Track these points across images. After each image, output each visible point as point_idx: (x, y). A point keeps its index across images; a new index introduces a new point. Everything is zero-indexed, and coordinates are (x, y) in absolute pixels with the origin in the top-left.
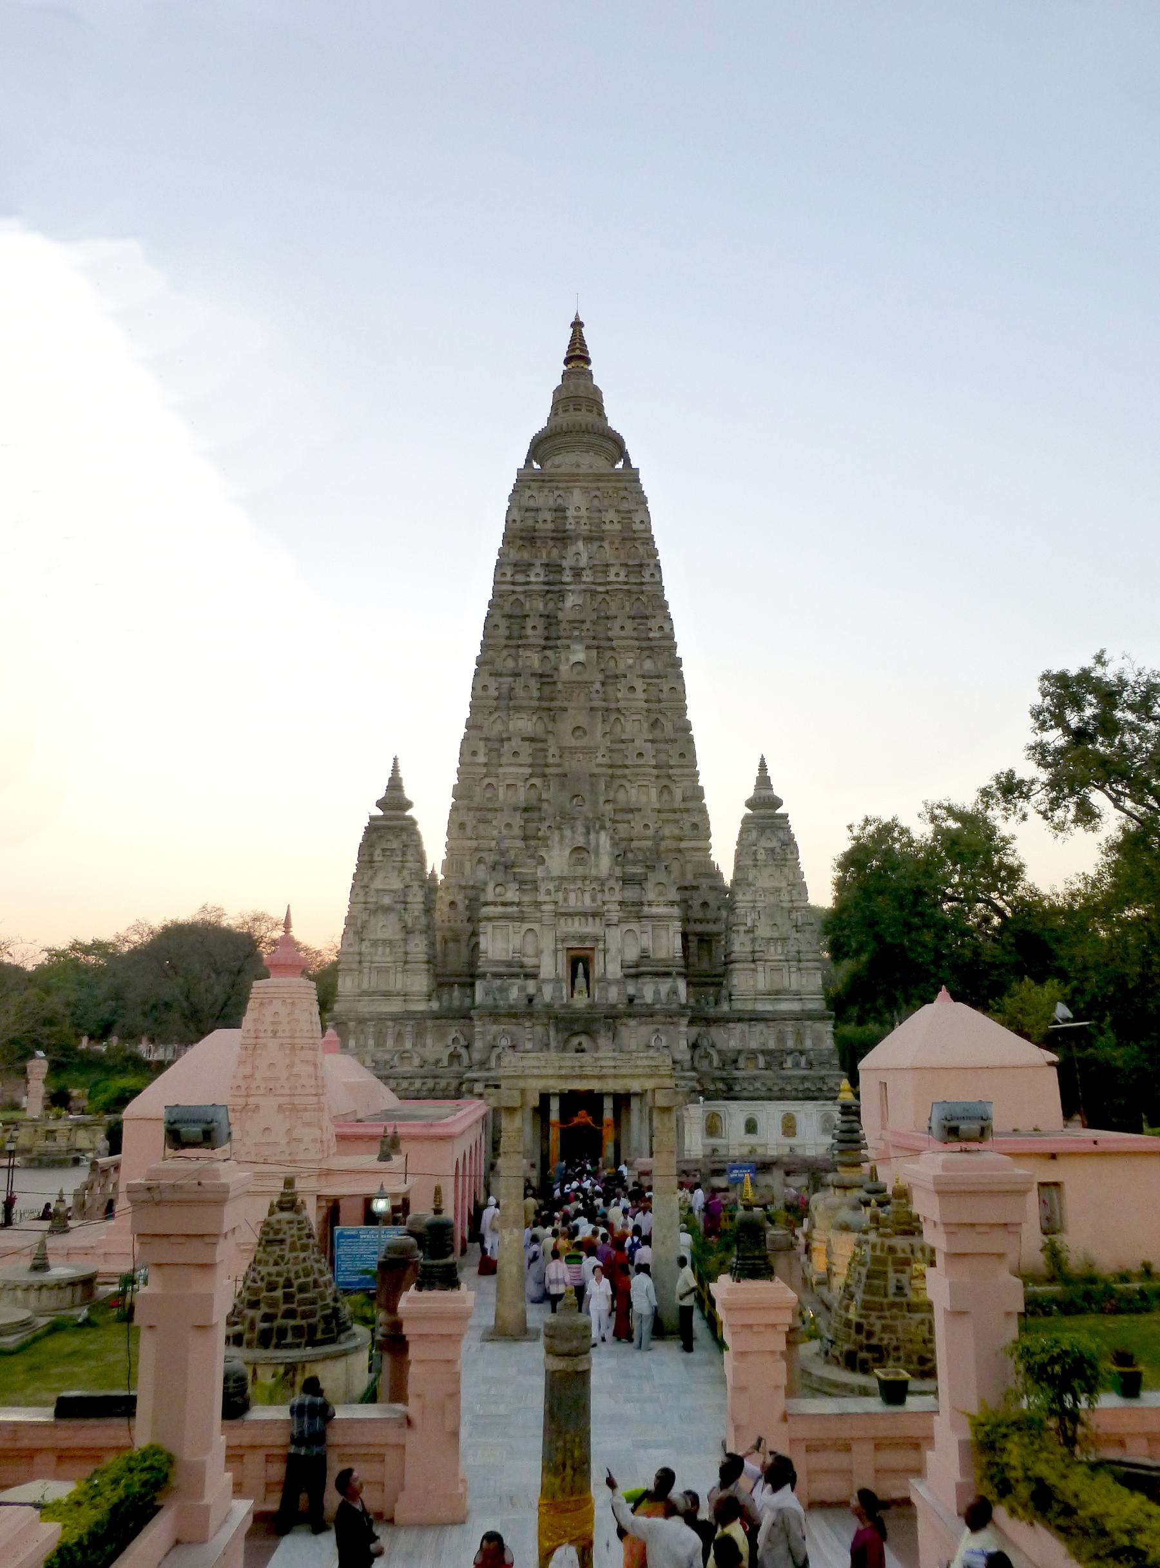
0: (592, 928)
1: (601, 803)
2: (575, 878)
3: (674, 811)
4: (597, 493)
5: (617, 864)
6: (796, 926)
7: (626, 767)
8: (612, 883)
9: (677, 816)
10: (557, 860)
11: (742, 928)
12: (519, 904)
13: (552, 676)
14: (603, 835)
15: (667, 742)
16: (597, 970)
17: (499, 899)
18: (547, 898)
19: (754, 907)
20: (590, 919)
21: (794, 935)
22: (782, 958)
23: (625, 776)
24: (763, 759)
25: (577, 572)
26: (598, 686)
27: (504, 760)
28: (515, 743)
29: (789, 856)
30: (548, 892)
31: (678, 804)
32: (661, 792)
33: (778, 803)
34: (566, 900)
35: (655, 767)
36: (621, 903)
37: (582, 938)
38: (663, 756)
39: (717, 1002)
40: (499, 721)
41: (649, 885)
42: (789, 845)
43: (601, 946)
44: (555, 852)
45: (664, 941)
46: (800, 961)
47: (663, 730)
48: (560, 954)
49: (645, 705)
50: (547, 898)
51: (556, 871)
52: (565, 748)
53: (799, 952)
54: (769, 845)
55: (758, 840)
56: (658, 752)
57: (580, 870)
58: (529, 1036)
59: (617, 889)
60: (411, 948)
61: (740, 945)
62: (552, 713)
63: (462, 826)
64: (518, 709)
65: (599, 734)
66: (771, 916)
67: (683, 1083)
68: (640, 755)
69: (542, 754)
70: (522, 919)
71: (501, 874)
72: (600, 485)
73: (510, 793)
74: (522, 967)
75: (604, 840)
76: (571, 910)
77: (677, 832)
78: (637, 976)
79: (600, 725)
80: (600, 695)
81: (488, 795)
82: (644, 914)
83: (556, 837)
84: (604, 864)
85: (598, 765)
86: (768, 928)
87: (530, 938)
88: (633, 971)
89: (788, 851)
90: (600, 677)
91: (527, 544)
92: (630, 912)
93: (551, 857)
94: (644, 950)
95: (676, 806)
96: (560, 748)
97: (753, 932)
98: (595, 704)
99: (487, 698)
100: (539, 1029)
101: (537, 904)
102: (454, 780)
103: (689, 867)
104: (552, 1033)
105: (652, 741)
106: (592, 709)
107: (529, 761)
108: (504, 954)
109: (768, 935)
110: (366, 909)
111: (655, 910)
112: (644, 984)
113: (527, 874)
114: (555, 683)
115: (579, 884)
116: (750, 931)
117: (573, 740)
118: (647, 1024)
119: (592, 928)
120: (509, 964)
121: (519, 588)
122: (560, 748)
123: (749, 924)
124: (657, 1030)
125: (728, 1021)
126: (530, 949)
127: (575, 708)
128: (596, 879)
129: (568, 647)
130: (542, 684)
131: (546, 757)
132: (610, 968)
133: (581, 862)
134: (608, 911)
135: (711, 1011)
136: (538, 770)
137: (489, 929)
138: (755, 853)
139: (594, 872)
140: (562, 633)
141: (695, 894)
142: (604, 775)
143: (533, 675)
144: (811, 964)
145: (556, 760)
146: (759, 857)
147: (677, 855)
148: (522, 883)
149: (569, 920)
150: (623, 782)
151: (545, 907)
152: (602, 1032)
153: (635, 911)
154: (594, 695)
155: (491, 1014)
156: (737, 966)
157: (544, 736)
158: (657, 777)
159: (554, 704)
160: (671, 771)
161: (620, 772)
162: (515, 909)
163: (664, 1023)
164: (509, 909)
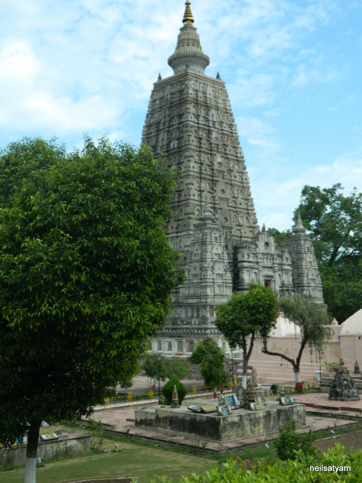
0: (270, 273)
4: (214, 89)
8: (276, 257)
13: (211, 166)
17: (248, 260)
22: (314, 285)
25: (214, 123)
37: (268, 276)
44: (261, 243)
51: (262, 252)
60: (227, 278)
72: (215, 86)
91: (196, 105)
95: (252, 225)
106: (226, 183)
110: (212, 261)
121: (196, 125)
129: (216, 155)
139: (271, 252)
140: (213, 149)
151: (260, 264)
164: (251, 264)
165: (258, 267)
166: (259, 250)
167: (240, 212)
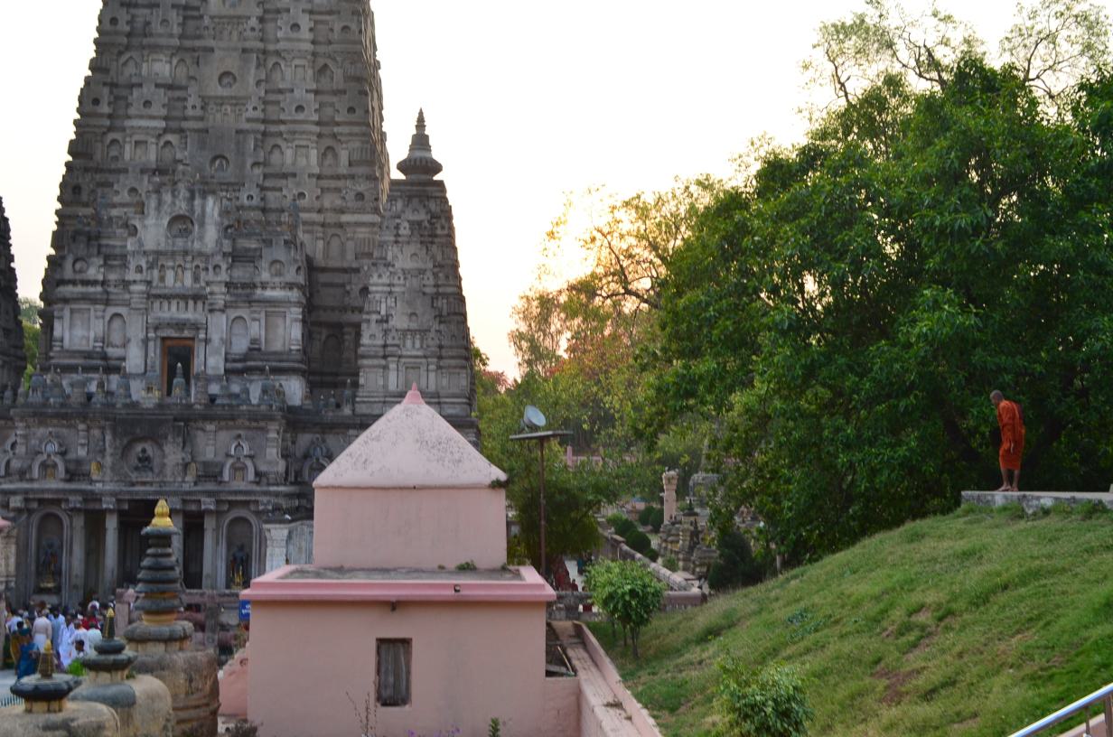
0: (191, 314)
1: (248, 165)
2: (173, 253)
3: (338, 177)
5: (225, 237)
6: (440, 316)
7: (283, 122)
8: (218, 259)
9: (340, 184)
10: (153, 232)
11: (374, 317)
12: (103, 283)
13: (197, 9)
14: (210, 201)
15: (336, 93)
16: (197, 365)
17: (78, 277)
18: (138, 277)
19: (390, 293)
20: (191, 303)
21: (436, 326)
22: (420, 353)
23: (281, 134)
24: (421, 113)
26: (253, 22)
27: (132, 111)
28: (148, 90)
29: (439, 232)
30: (139, 269)
31: (343, 170)
32: (324, 155)
33: (437, 168)
34: (162, 279)
35: (318, 123)
36: (227, 285)
37: (180, 325)
38: (329, 111)
39: (338, 406)
40: (131, 64)
41: (264, 264)
42: (446, 214)
43: (202, 336)
44: (150, 221)
45: (280, 331)
46: (440, 358)
47: (332, 79)
48: (151, 344)
49: (309, 47)
50: (138, 277)
51: (150, 245)
52: (210, 98)
53: (441, 347)
54: (416, 217)
55: (404, 212)
56: (322, 105)
57: (180, 243)
58: (83, 441)
59: (224, 266)
61: (370, 337)
62: (196, 54)
63: (77, 189)
64: (155, 48)
65: (252, 81)
66: (409, 303)
67: (265, 499)
68: (300, 108)
69: (179, 104)
70: (107, 303)
71: (82, 246)
73: (139, 151)
74: (105, 357)
75: (212, 207)
76: (166, 291)
77: (338, 202)
78: (239, 372)
79: (253, 71)
80: (256, 34)
81: (114, 153)
82: (256, 297)
83: (153, 203)
84: (210, 236)
85: (248, 120)
86: (405, 318)
87: (117, 324)
88: (239, 365)
89: (438, 226)
90: (259, 12)
92: (240, 295)
93: (145, 227)
94: (254, 341)
96: (203, 98)
97: (387, 321)
98: (248, 45)
99: (116, 33)
100: (96, 432)
101: (126, 284)
102: (70, 133)
103: (350, 245)
104: (108, 437)
105: (316, 92)
106: (244, 51)
107: (164, 112)
108: (84, 342)
109: (405, 326)
111: (269, 293)
112: (251, 381)
113: (114, 247)
114: (201, 17)
115: (179, 261)
116: (385, 320)
117: (219, 87)
118: (228, 428)
119: (191, 314)
120: (88, 355)
122: (203, 98)
123: (383, 312)
124: (239, 436)
125: (348, 427)
126: (116, 338)
127: (224, 49)
128: (200, 254)
130: (185, 18)
131: (185, 108)
132: (211, 361)
133: (186, 233)
134: (212, 293)
135: (329, 415)
136: (173, 124)
137: (67, 313)
138: (397, 227)
139: (197, 245)
141: (354, 278)
142: (255, 132)
143: (174, 6)
144: (453, 362)
145: (198, 112)
146: (402, 231)
147: (338, 231)
148: (107, 258)
149: (166, 304)
150: (279, 141)
151: (134, 288)
152: (170, 438)
153: (243, 293)
154: (249, 33)
155: (35, 415)
156: (365, 362)
157: (184, 83)
158: (320, 136)
159: (197, 43)
160: (336, 129)
161: (273, 128)
162: (99, 289)
163: (249, 428)
164: (91, 289)
165: (127, 296)
166: (141, 244)
167: (294, 133)
